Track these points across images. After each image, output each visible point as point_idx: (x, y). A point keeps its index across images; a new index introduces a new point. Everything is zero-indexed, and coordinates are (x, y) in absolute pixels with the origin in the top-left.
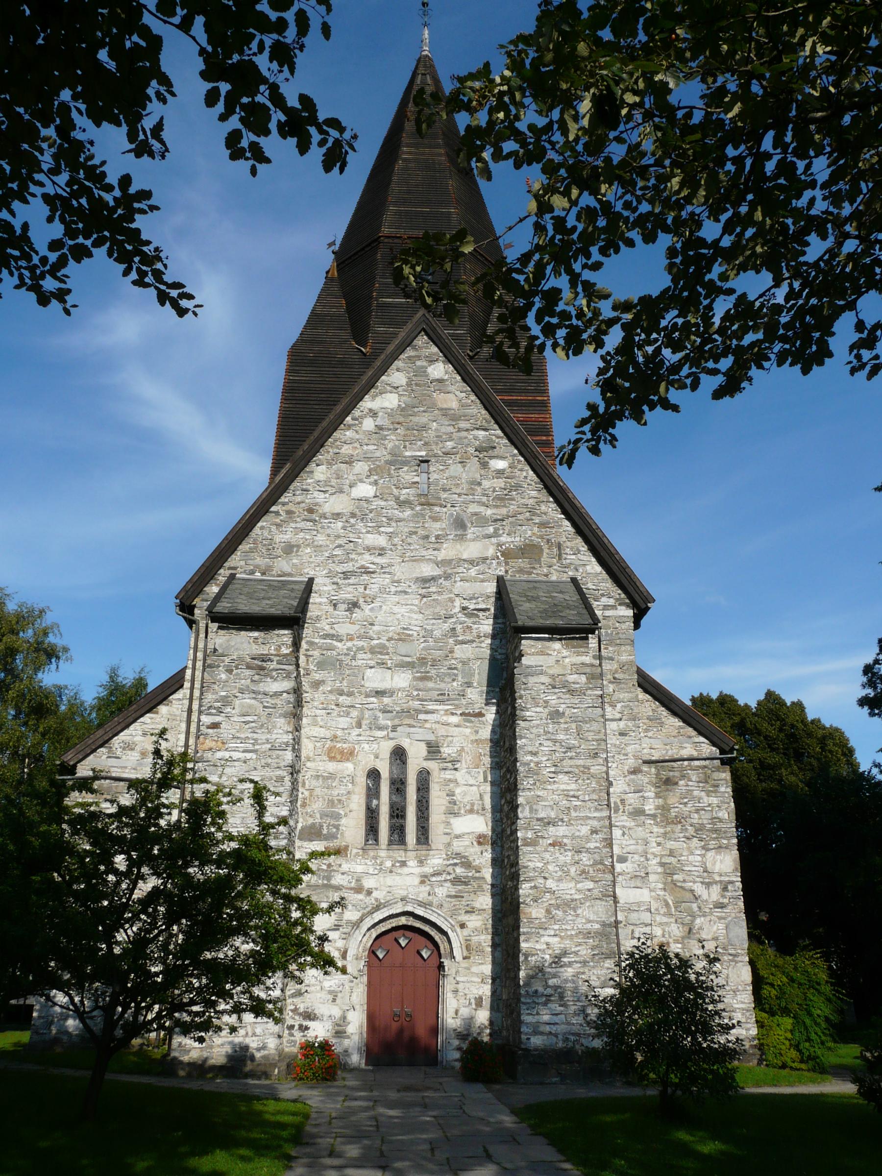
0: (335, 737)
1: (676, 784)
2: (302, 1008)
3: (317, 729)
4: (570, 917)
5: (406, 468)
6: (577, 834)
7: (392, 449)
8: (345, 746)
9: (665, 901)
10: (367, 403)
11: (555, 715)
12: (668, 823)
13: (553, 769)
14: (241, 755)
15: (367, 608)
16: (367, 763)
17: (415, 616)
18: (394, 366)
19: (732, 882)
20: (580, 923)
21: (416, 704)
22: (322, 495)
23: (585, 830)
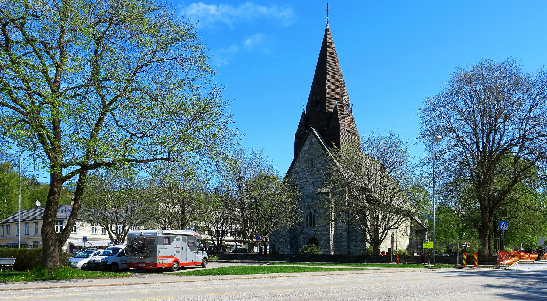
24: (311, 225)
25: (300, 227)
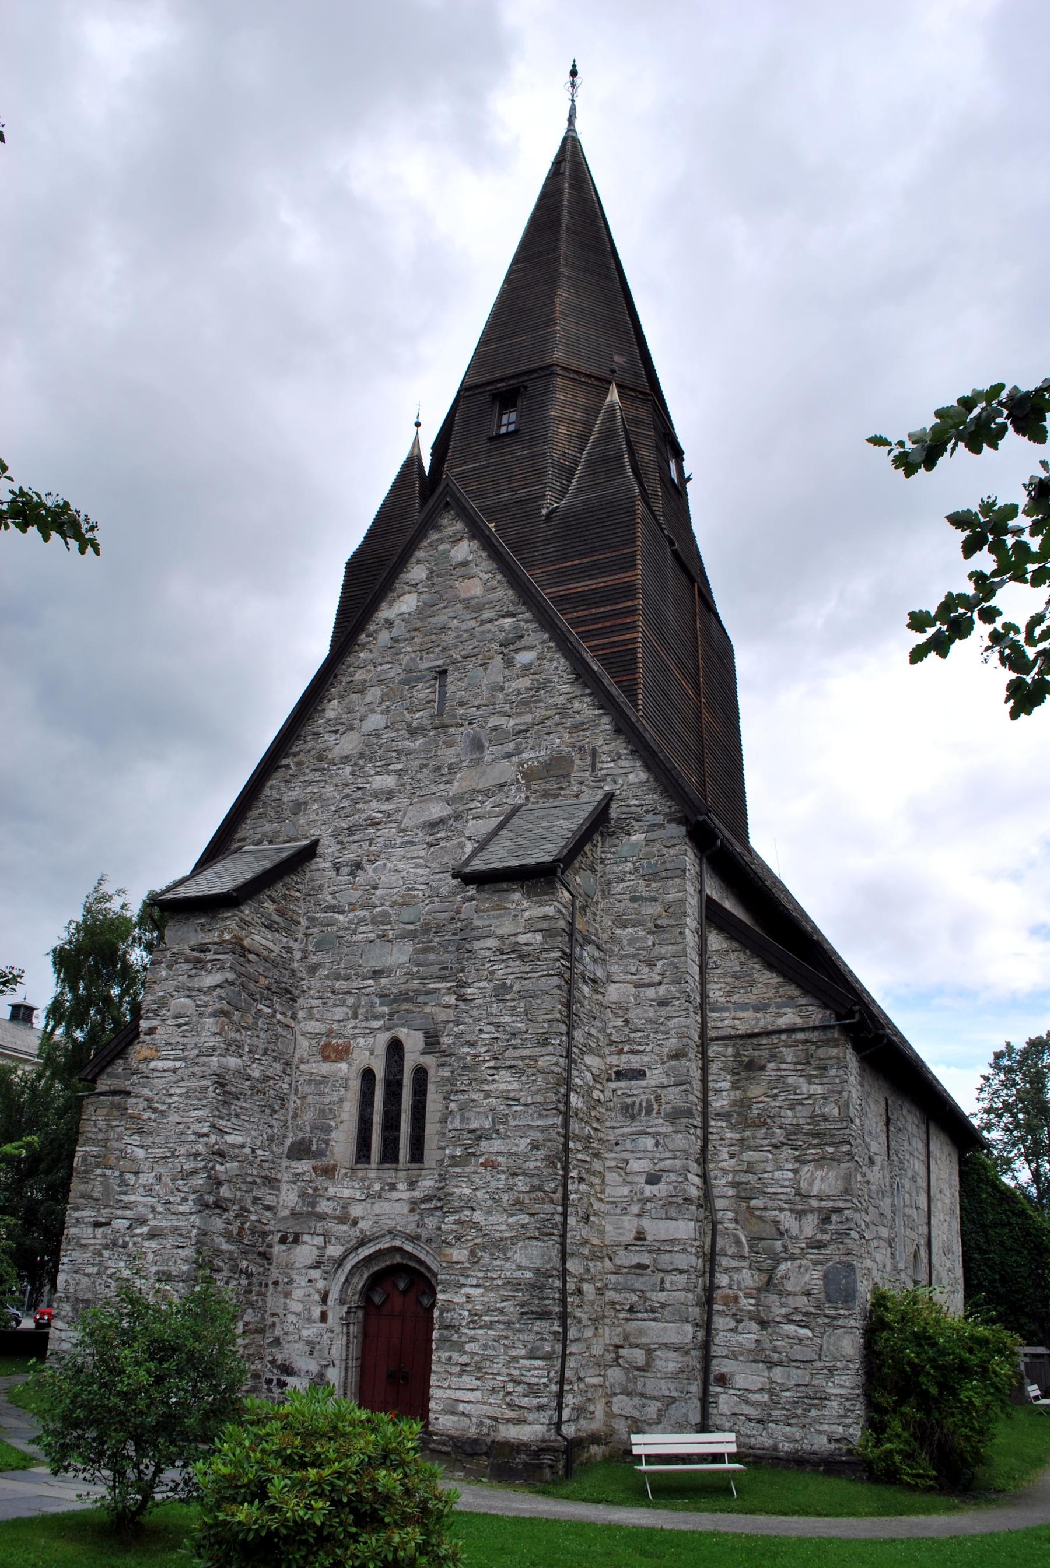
0: (331, 1031)
1: (763, 1068)
2: (280, 1358)
3: (313, 1023)
4: (498, 1262)
5: (421, 685)
6: (515, 1149)
7: (407, 665)
8: (340, 1041)
9: (736, 1237)
10: (385, 612)
11: (501, 990)
12: (747, 1126)
13: (492, 1064)
14: (169, 1064)
15: (369, 868)
16: (360, 1063)
17: (421, 871)
18: (413, 560)
19: (838, 1210)
20: (509, 1271)
21: (415, 984)
22: (334, 737)
23: (523, 1144)
24: (390, 1155)
25: (303, 1166)
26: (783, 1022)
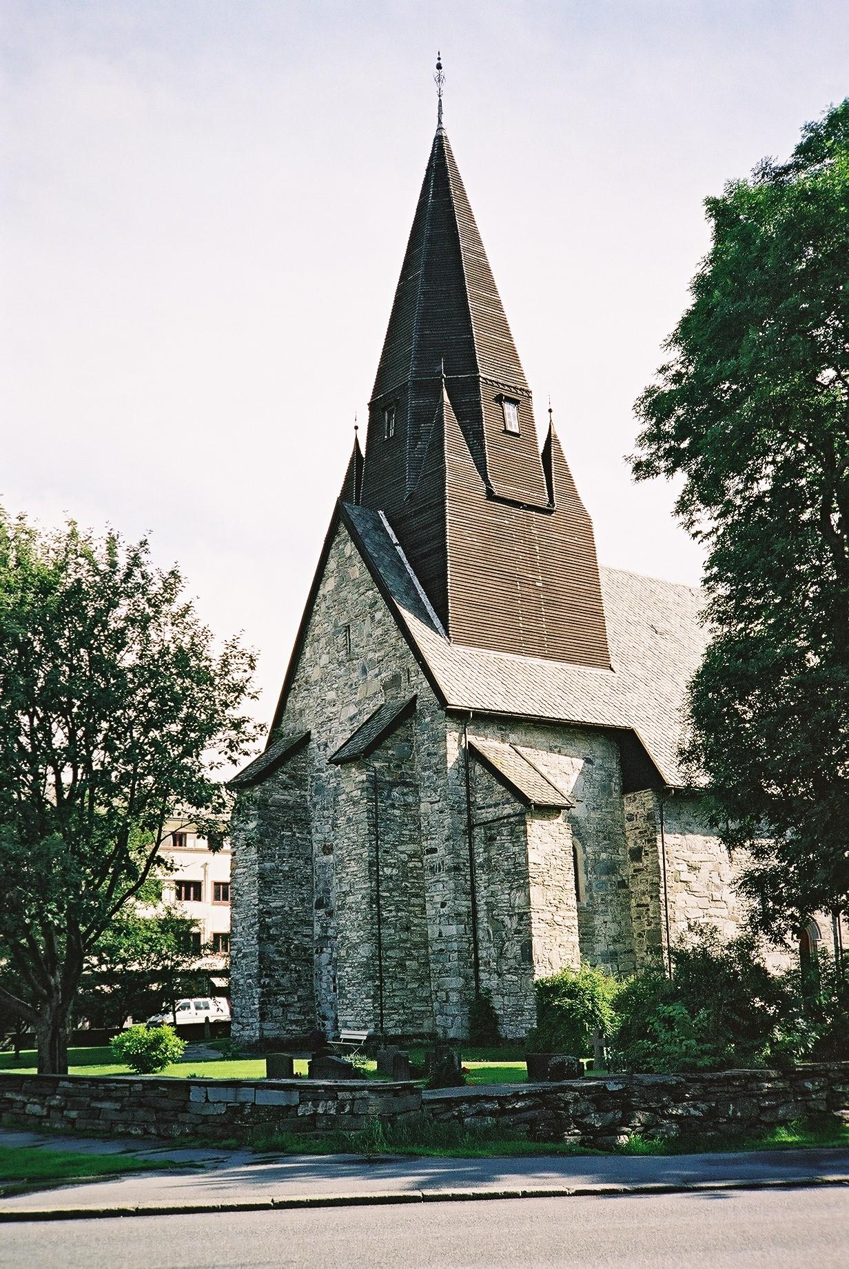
11: (349, 820)
25: (321, 912)
26: (506, 812)
